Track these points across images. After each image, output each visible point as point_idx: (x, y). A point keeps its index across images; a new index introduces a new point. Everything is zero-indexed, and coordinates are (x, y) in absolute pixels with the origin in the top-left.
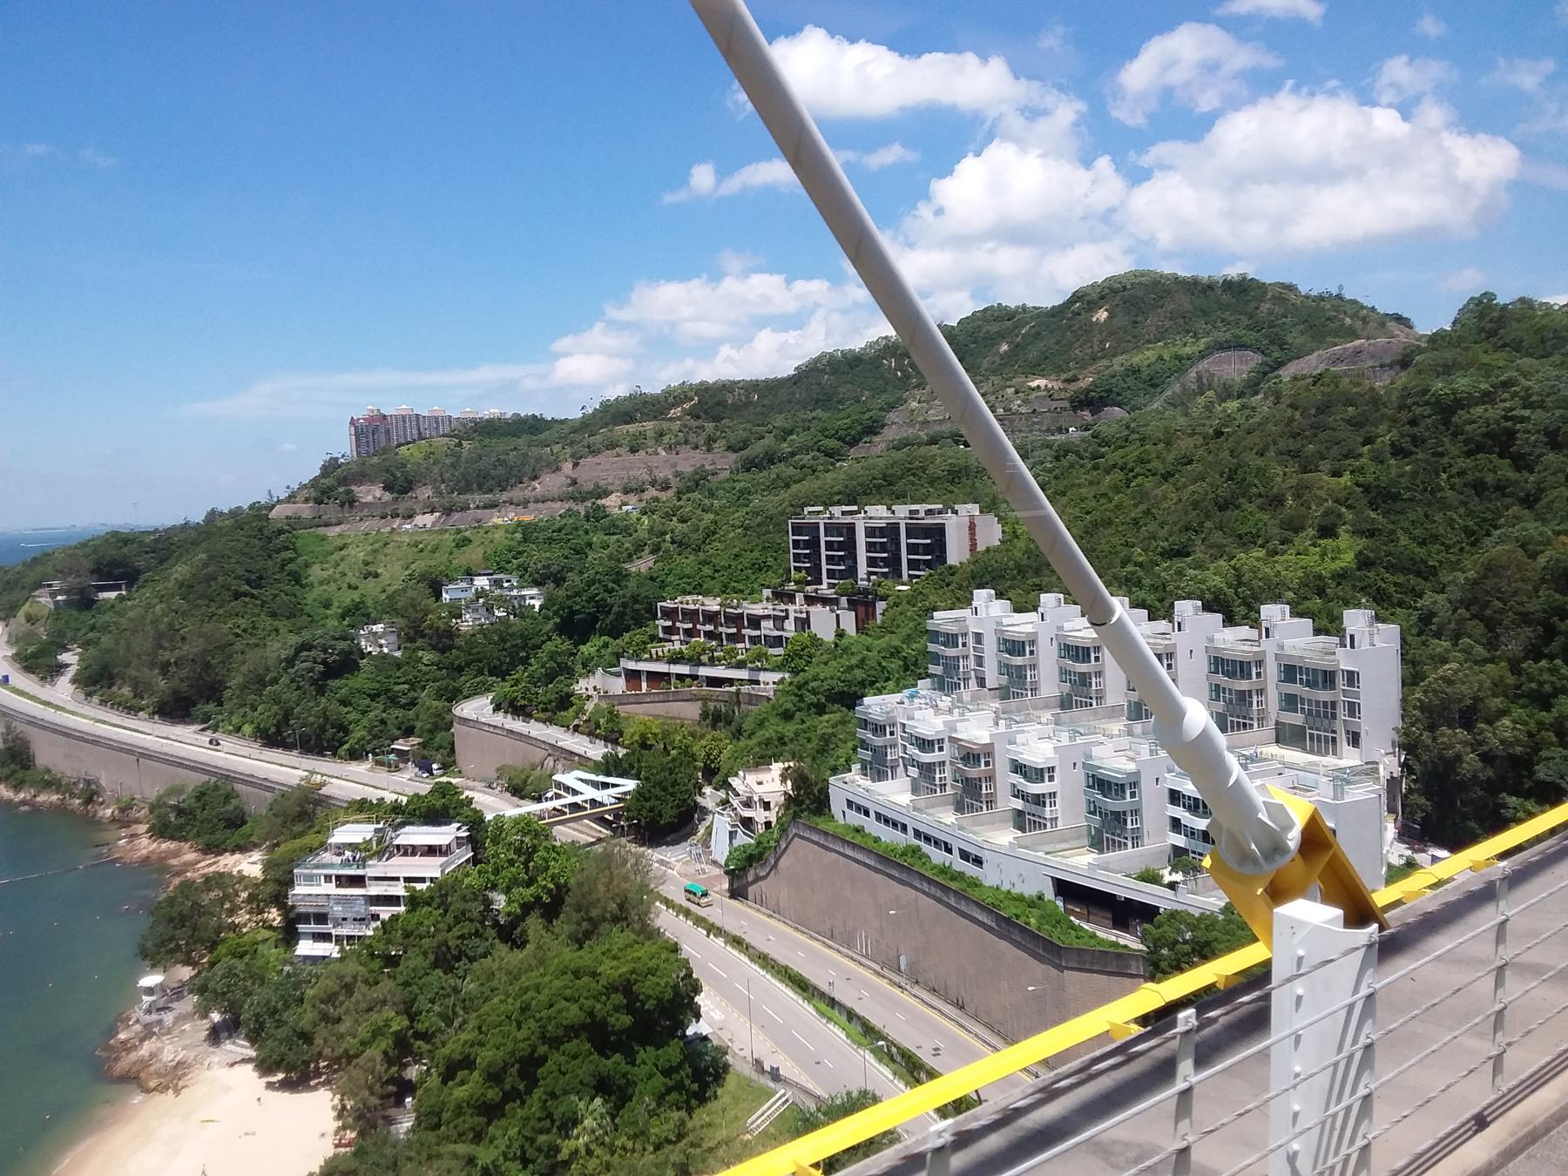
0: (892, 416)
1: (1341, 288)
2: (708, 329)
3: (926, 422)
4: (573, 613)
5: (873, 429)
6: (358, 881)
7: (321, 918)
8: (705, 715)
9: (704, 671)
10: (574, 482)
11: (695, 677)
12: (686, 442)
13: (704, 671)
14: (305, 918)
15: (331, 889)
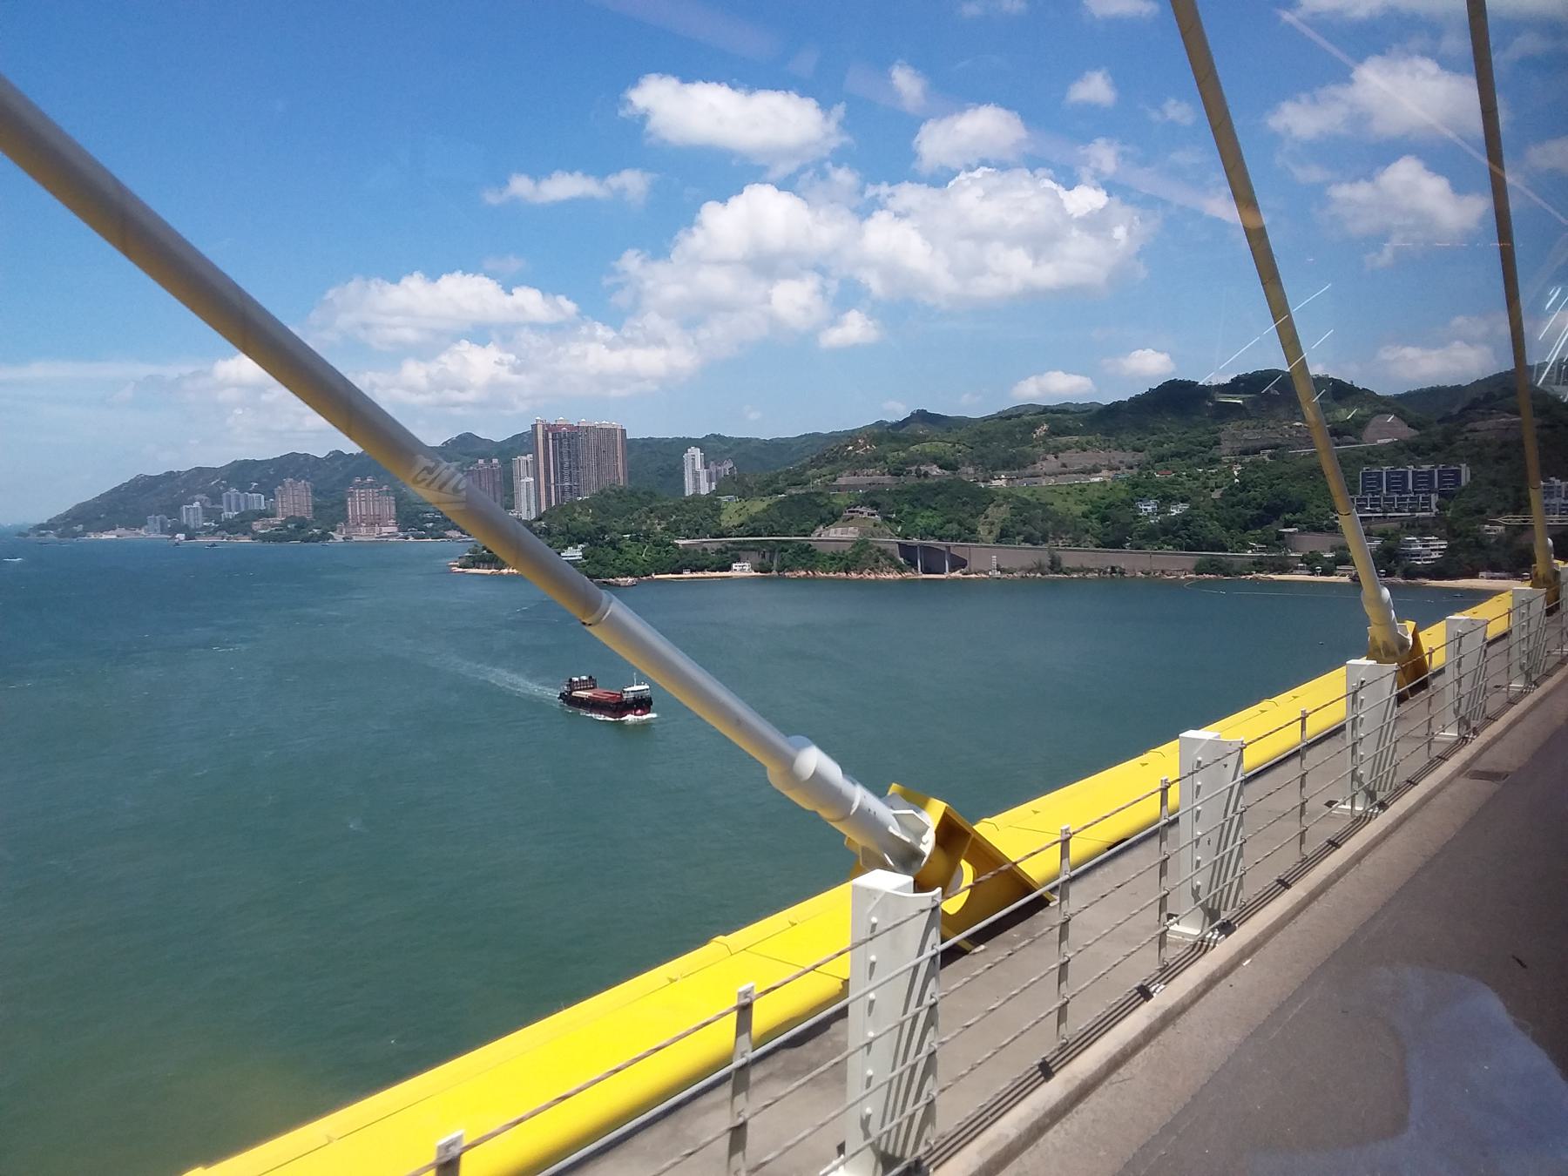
0: (1221, 435)
1: (1352, 382)
2: (409, 335)
3: (1246, 440)
4: (1275, 504)
5: (1217, 443)
6: (1428, 546)
7: (1419, 556)
8: (1402, 526)
9: (1389, 514)
10: (1064, 465)
11: (1384, 517)
12: (1109, 447)
13: (1389, 514)
14: (1414, 556)
15: (1421, 548)
